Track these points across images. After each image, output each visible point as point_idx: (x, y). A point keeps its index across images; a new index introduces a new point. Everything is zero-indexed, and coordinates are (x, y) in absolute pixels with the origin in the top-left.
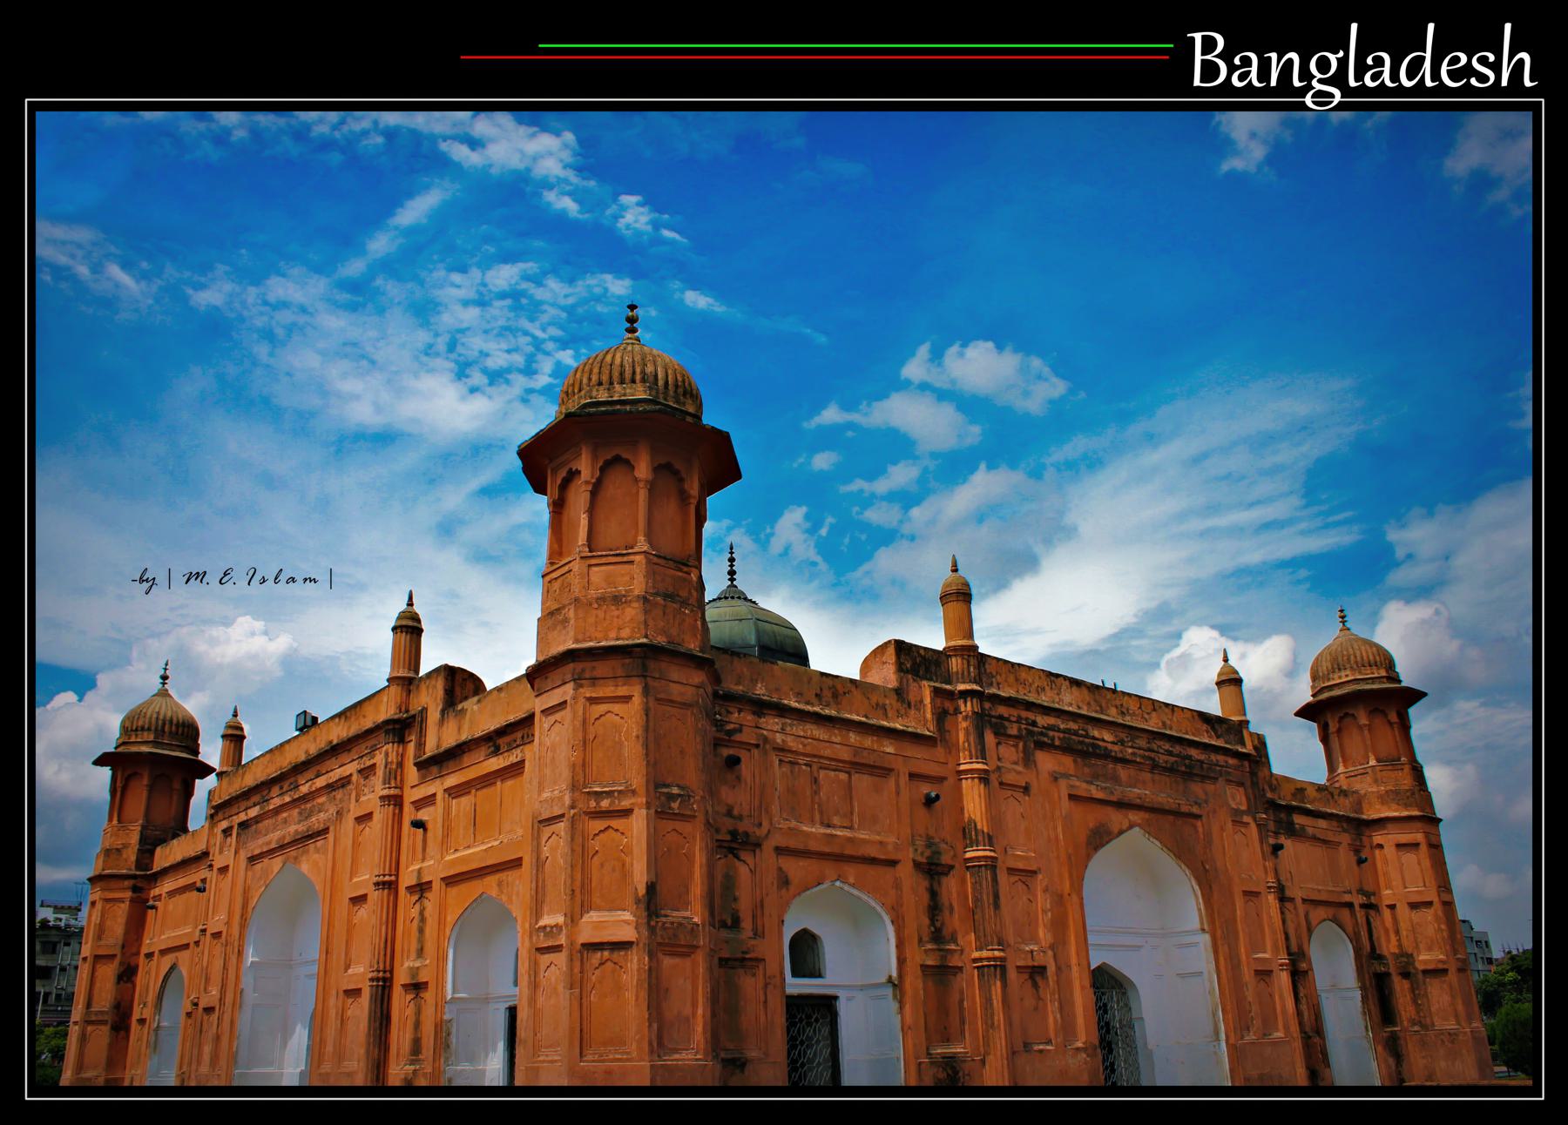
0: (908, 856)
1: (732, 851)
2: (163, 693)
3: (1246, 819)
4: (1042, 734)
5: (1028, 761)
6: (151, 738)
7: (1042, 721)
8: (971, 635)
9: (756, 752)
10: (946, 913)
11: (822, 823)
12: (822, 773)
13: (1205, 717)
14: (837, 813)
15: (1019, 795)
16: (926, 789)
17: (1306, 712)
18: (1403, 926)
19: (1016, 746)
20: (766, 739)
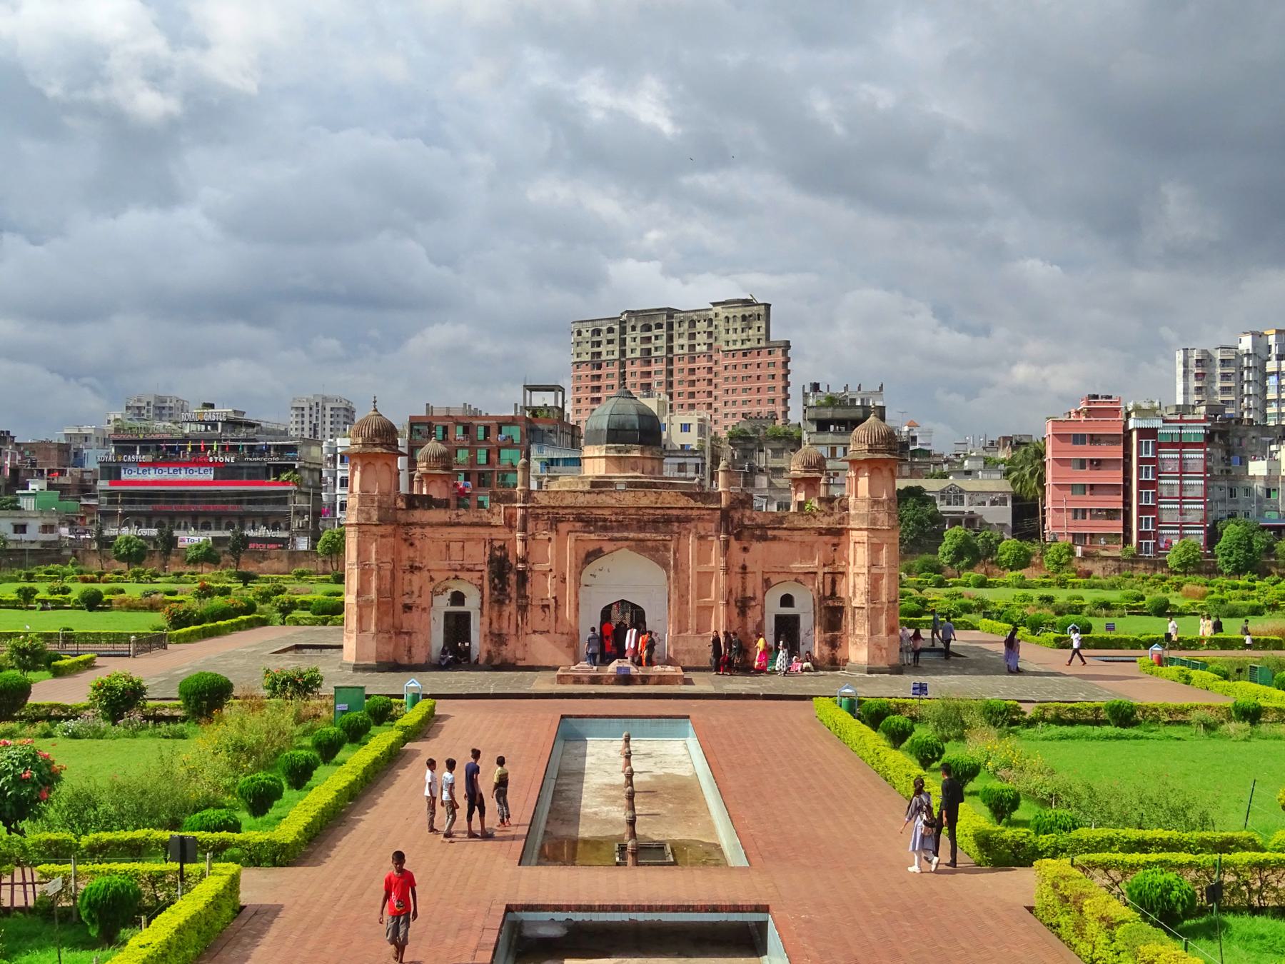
0: (487, 570)
7: (561, 512)
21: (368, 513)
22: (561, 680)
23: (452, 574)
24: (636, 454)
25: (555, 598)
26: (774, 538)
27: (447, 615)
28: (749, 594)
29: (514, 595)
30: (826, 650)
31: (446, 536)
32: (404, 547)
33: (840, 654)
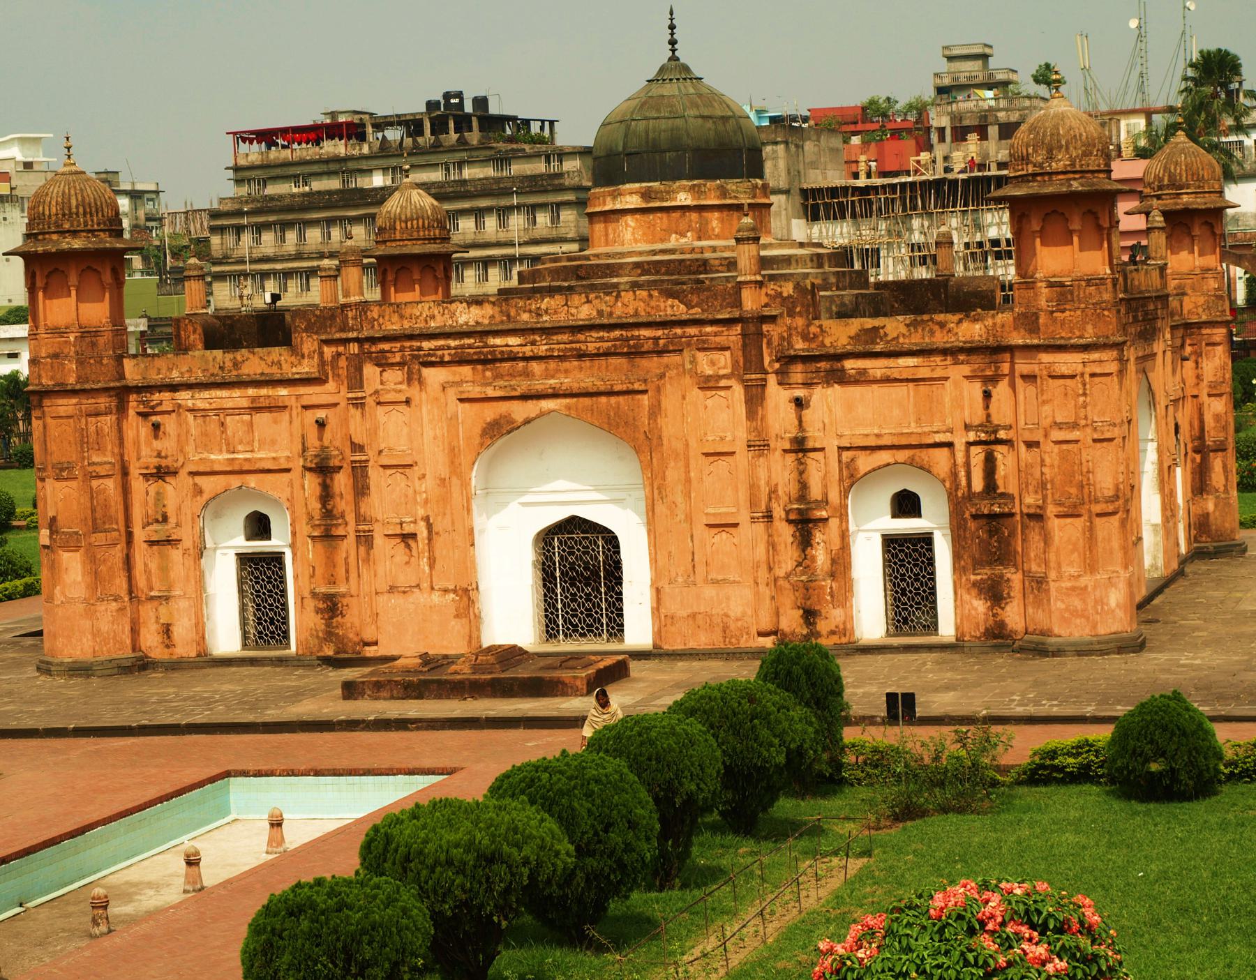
1: (160, 478)
3: (723, 383)
4: (429, 355)
7: (426, 345)
9: (174, 415)
10: (338, 499)
11: (229, 452)
12: (228, 418)
14: (241, 442)
15: (403, 408)
16: (321, 414)
20: (180, 406)
22: (350, 691)
24: (684, 198)
26: (862, 379)
27: (246, 561)
29: (350, 518)
30: (980, 606)
32: (145, 430)
33: (1013, 615)
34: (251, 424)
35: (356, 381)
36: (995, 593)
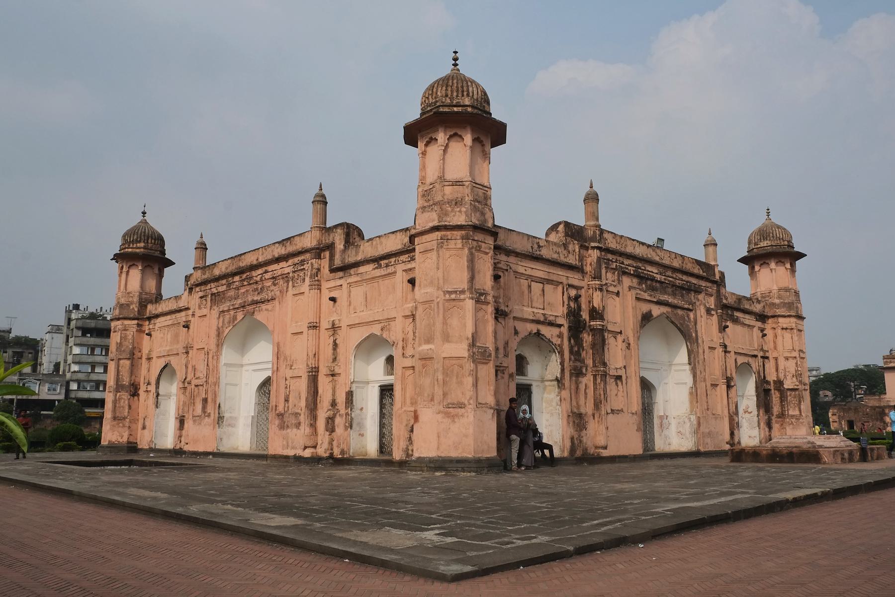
2: (146, 223)
3: (713, 312)
5: (620, 282)
6: (142, 245)
8: (597, 219)
13: (698, 262)
15: (614, 297)
16: (573, 293)
17: (743, 260)
18: (781, 367)
19: (614, 273)
21: (483, 214)
23: (533, 328)
25: (625, 367)
28: (729, 375)
31: (529, 272)
34: (543, 290)
35: (597, 277)
36: (769, 425)
